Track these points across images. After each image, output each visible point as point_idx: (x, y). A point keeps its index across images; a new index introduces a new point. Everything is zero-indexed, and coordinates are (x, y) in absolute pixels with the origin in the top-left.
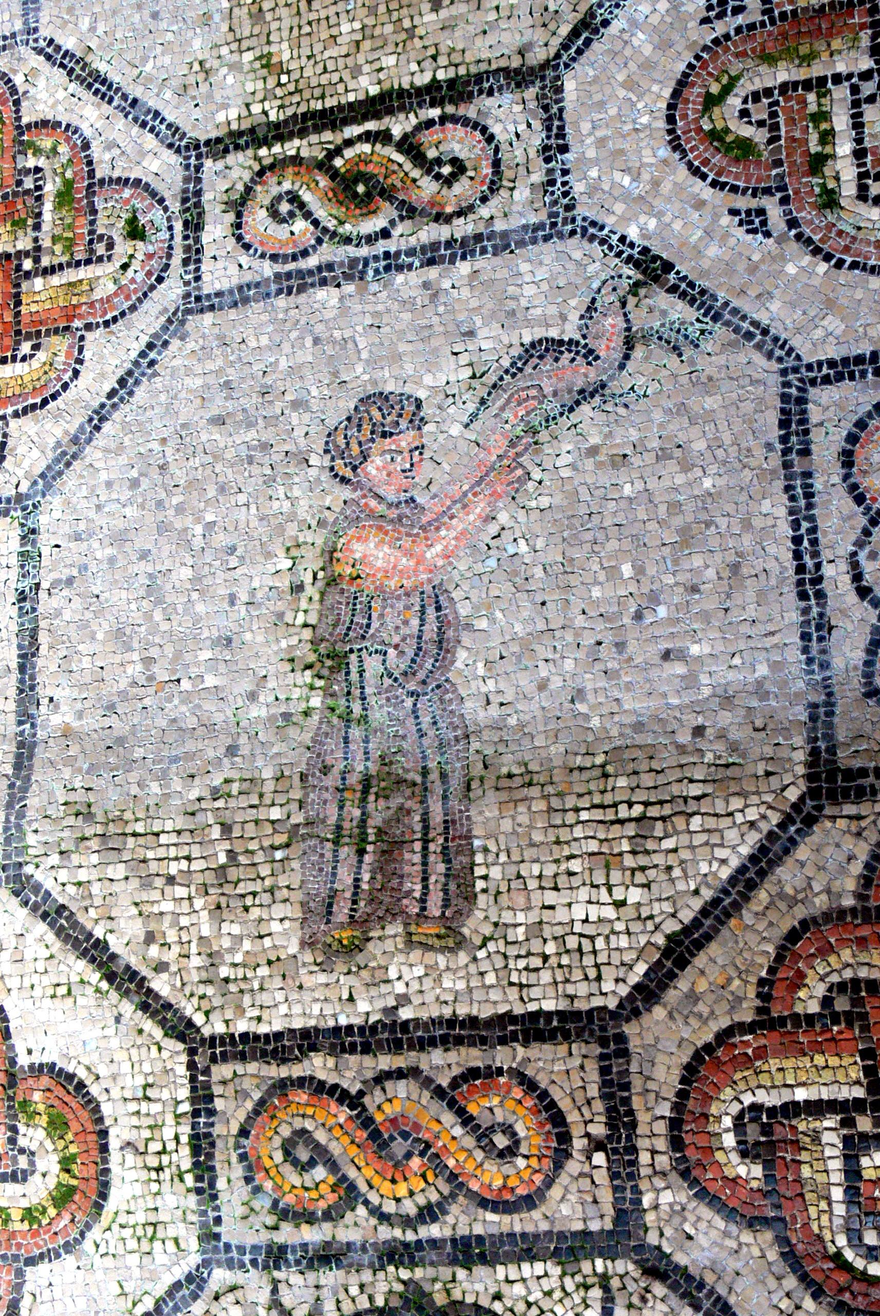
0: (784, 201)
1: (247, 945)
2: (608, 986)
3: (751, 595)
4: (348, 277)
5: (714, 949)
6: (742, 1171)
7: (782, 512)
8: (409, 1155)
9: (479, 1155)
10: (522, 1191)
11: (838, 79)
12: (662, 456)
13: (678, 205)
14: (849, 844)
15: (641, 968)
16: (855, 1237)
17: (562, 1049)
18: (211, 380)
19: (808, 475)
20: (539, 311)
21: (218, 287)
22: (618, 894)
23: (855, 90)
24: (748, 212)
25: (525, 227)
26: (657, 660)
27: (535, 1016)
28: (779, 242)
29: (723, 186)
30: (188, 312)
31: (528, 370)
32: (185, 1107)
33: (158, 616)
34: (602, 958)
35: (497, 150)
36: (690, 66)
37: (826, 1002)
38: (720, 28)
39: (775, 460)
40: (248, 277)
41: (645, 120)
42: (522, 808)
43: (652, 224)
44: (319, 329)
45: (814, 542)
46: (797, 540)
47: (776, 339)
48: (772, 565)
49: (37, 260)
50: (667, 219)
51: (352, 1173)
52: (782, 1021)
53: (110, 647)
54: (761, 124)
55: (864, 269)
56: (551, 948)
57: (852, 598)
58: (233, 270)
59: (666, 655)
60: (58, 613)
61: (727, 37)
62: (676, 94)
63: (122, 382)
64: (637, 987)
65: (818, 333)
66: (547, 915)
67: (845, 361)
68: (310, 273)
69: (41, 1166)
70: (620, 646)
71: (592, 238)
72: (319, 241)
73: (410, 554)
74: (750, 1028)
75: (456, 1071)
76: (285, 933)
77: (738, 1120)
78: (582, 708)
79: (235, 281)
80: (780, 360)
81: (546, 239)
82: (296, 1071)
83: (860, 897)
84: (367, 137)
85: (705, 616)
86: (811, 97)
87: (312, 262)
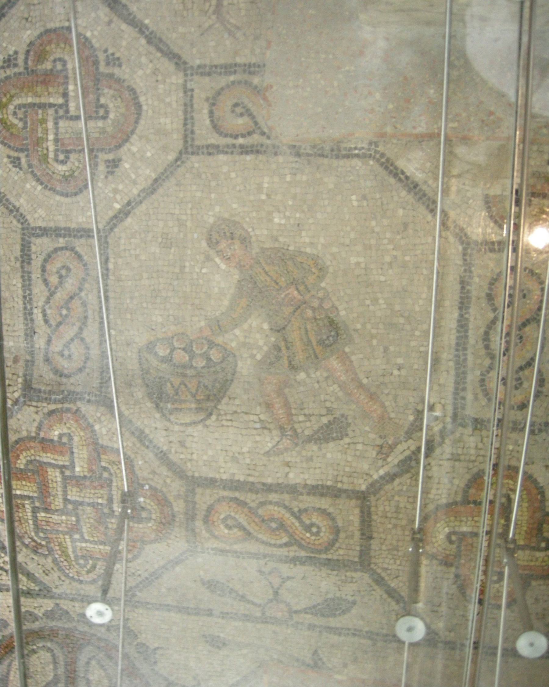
0: (27, 156)
7: (20, 285)
11: (51, 105)
14: (35, 416)
16: (37, 534)
19: (30, 273)
24: (14, 158)
28: (25, 173)
38: (9, 72)
39: (18, 264)
45: (31, 299)
46: (25, 297)
47: (21, 215)
48: (16, 305)
54: (21, 119)
55: (54, 191)
57: (42, 323)
65: (36, 215)
80: (22, 224)
86: (40, 112)
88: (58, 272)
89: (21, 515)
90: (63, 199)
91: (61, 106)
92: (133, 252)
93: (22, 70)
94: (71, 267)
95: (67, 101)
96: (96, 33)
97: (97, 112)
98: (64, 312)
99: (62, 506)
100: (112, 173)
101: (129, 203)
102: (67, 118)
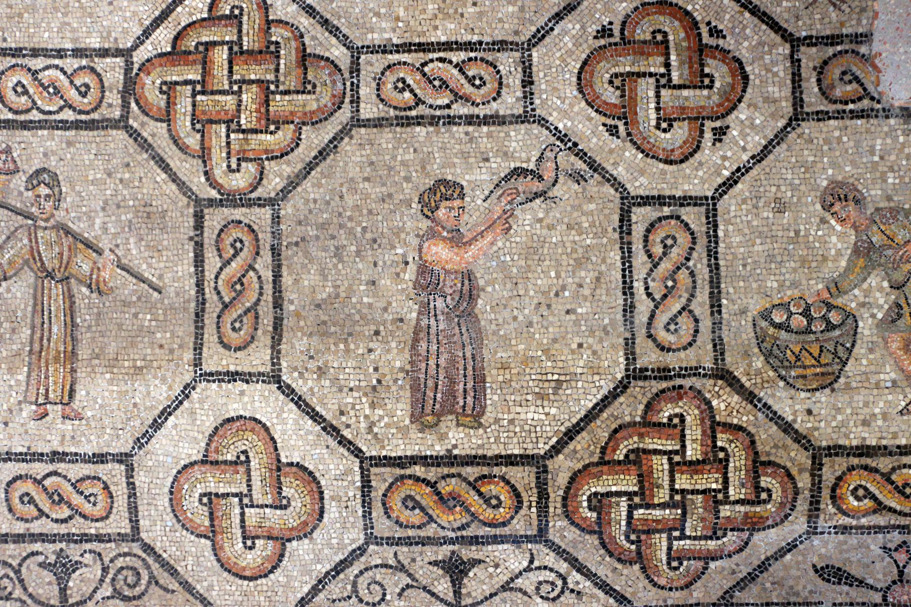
0: (626, 124)
2: (541, 445)
3: (604, 292)
4: (431, 124)
5: (584, 434)
6: (589, 515)
7: (618, 258)
8: (455, 506)
9: (485, 506)
10: (501, 520)
12: (569, 227)
15: (555, 440)
17: (521, 468)
21: (368, 116)
22: (547, 410)
23: (658, 81)
25: (513, 115)
26: (563, 313)
29: (600, 113)
30: (353, 126)
32: (359, 484)
34: (539, 434)
37: (627, 456)
39: (617, 236)
40: (382, 115)
42: (507, 371)
43: (569, 124)
44: (416, 145)
45: (631, 272)
46: (624, 270)
48: (613, 278)
56: (518, 429)
57: (644, 297)
58: (375, 110)
59: (568, 312)
61: (605, 46)
64: (553, 447)
65: (637, 184)
66: (517, 416)
67: (647, 197)
68: (413, 118)
71: (542, 126)
72: (417, 104)
73: (457, 254)
75: (476, 475)
77: (589, 497)
78: (532, 330)
79: (376, 116)
81: (523, 122)
83: (642, 417)
85: (585, 299)
87: (414, 113)
88: (662, 242)
90: (666, 167)
91: (662, 75)
92: (744, 218)
94: (677, 235)
95: (669, 71)
96: (697, 7)
97: (702, 82)
98: (670, 283)
99: (667, 498)
100: (720, 140)
101: (738, 169)
102: (670, 87)
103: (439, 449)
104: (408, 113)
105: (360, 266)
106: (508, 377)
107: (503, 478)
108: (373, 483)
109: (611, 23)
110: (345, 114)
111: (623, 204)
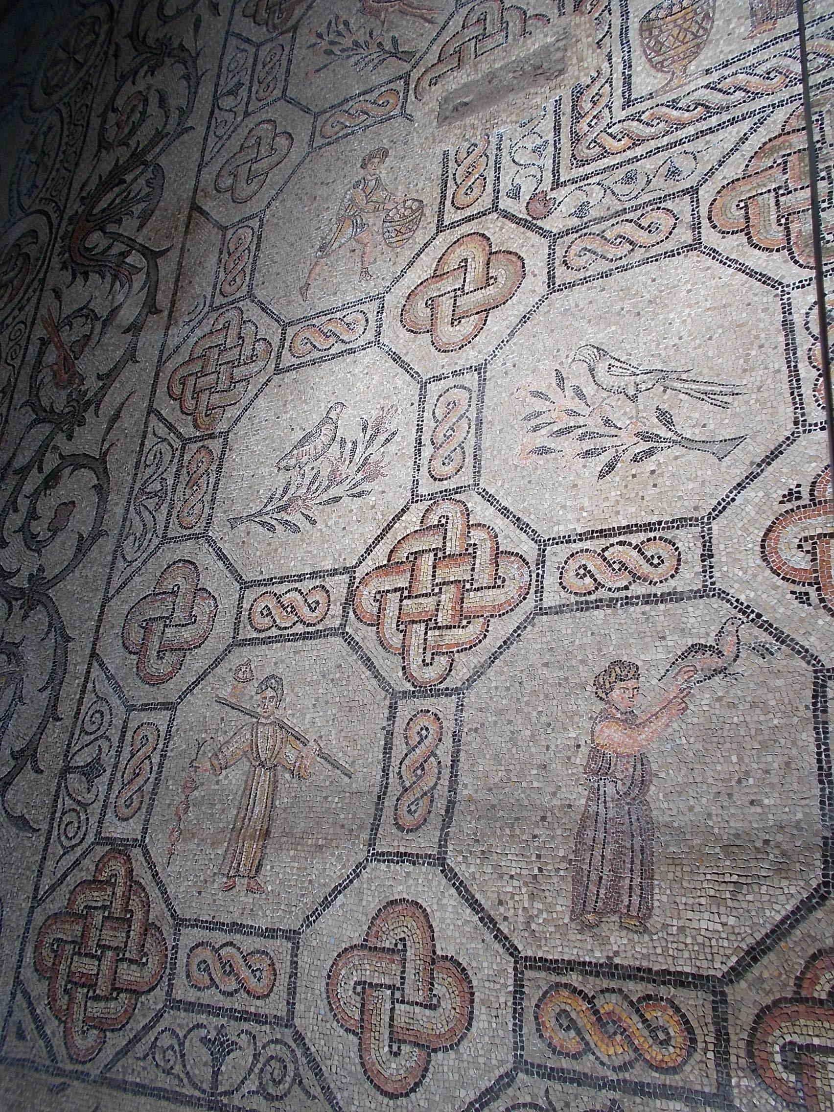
1: (545, 915)
3: (795, 779)
4: (608, 606)
5: (772, 956)
6: (785, 1076)
7: (812, 740)
8: (615, 1033)
9: (651, 1041)
10: (671, 1064)
12: (753, 705)
13: (764, 587)
15: (734, 959)
17: (693, 994)
18: (544, 646)
19: (826, 723)
20: (695, 631)
22: (724, 919)
24: (800, 593)
25: (691, 591)
27: (680, 973)
29: (788, 580)
30: (536, 614)
31: (690, 657)
32: (511, 989)
33: (514, 750)
34: (715, 950)
35: (679, 554)
36: (774, 523)
40: (564, 602)
41: (750, 546)
42: (678, 868)
43: (752, 595)
44: (594, 628)
45: (827, 756)
46: (819, 754)
47: (812, 655)
49: (472, 584)
50: (759, 593)
51: (587, 1037)
52: (807, 1000)
53: (492, 762)
59: (752, 803)
60: (470, 743)
61: (792, 510)
62: (766, 535)
63: (505, 642)
64: (732, 968)
66: (688, 923)
69: (443, 1004)
70: (730, 795)
71: (723, 599)
72: (597, 588)
74: (791, 1001)
75: (640, 995)
76: (563, 912)
77: (783, 1048)
80: (814, 665)
81: (701, 597)
82: (564, 980)
84: (621, 543)
87: (593, 597)
89: (819, 1083)
93: (807, 502)
103: (598, 956)
104: (588, 598)
105: (533, 750)
106: (679, 874)
107: (671, 1002)
108: (526, 990)
109: (799, 486)
110: (530, 603)
111: (816, 678)
